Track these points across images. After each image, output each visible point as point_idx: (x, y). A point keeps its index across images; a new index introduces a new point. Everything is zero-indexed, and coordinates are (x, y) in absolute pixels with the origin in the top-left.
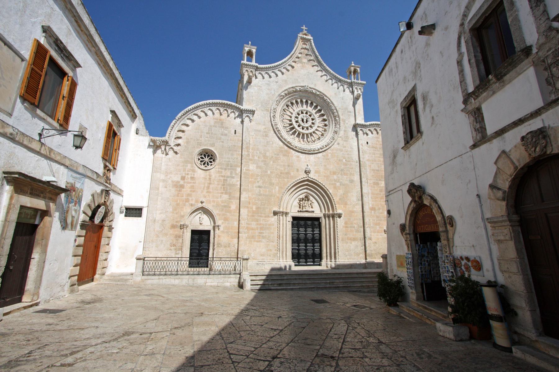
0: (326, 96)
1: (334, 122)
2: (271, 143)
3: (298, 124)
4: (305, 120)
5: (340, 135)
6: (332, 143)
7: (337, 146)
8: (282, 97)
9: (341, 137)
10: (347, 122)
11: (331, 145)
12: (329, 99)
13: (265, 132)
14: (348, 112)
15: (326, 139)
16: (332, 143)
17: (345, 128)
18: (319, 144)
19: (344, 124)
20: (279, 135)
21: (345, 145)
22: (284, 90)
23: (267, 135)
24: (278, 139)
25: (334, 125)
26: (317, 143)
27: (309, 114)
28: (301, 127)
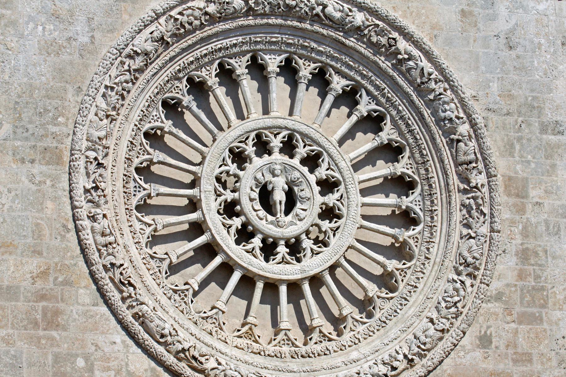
0: (408, 37)
1: (457, 198)
2: (81, 363)
3: (237, 222)
4: (279, 196)
5: (496, 285)
6: (446, 343)
7: (478, 354)
8: (139, 62)
9: (498, 297)
10: (534, 193)
11: (437, 353)
12: (428, 55)
13: (43, 297)
14: (544, 129)
15: (410, 310)
16: (446, 343)
17: (525, 234)
18: (365, 348)
19: (521, 210)
20: (122, 308)
21: (523, 344)
22: (147, 13)
23: (57, 313)
24: (120, 336)
25: (458, 216)
26: (356, 342)
27: (302, 151)
28: (257, 242)
